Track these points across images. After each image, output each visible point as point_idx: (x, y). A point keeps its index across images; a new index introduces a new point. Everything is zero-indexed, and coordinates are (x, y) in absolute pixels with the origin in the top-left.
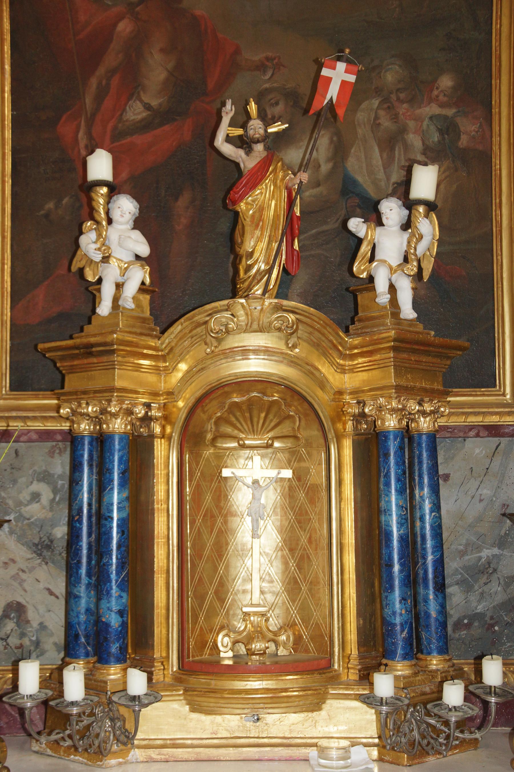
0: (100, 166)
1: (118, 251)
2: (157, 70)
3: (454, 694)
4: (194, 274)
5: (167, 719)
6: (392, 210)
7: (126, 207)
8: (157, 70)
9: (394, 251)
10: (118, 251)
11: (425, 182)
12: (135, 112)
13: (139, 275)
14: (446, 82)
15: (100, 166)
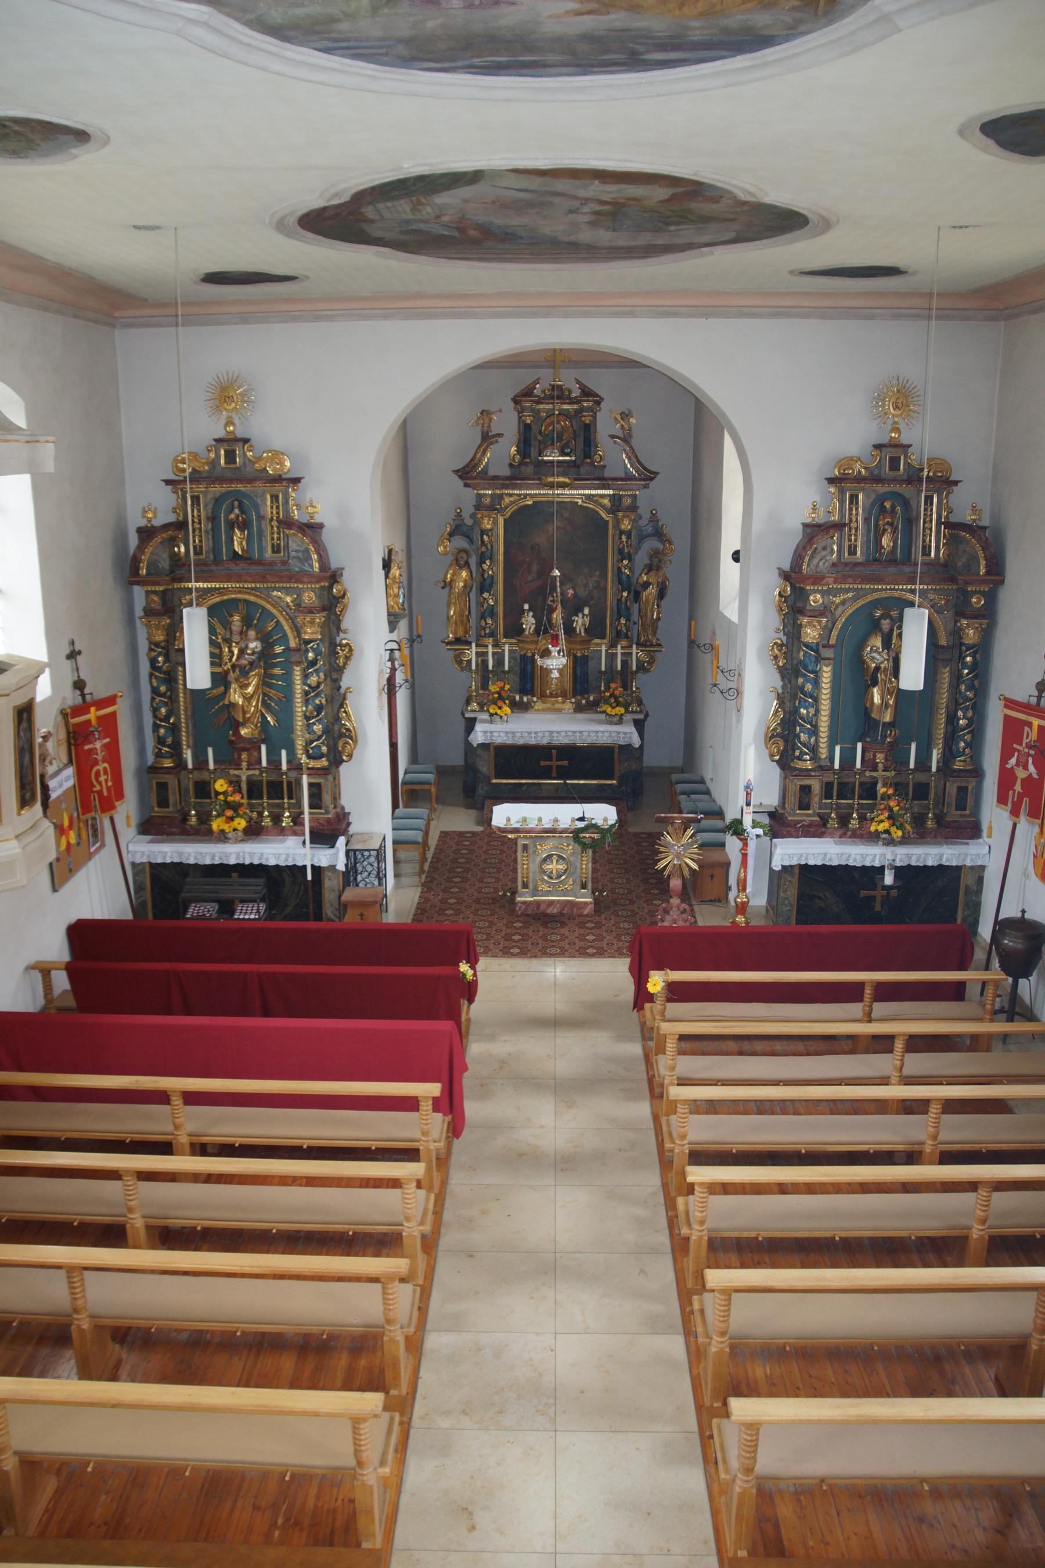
0: (526, 607)
1: (529, 622)
2: (535, 568)
3: (584, 702)
4: (543, 628)
5: (539, 705)
6: (580, 615)
7: (531, 614)
8: (535, 568)
9: (580, 622)
10: (529, 622)
11: (586, 611)
12: (530, 579)
13: (533, 627)
14: (598, 573)
15: (526, 607)
